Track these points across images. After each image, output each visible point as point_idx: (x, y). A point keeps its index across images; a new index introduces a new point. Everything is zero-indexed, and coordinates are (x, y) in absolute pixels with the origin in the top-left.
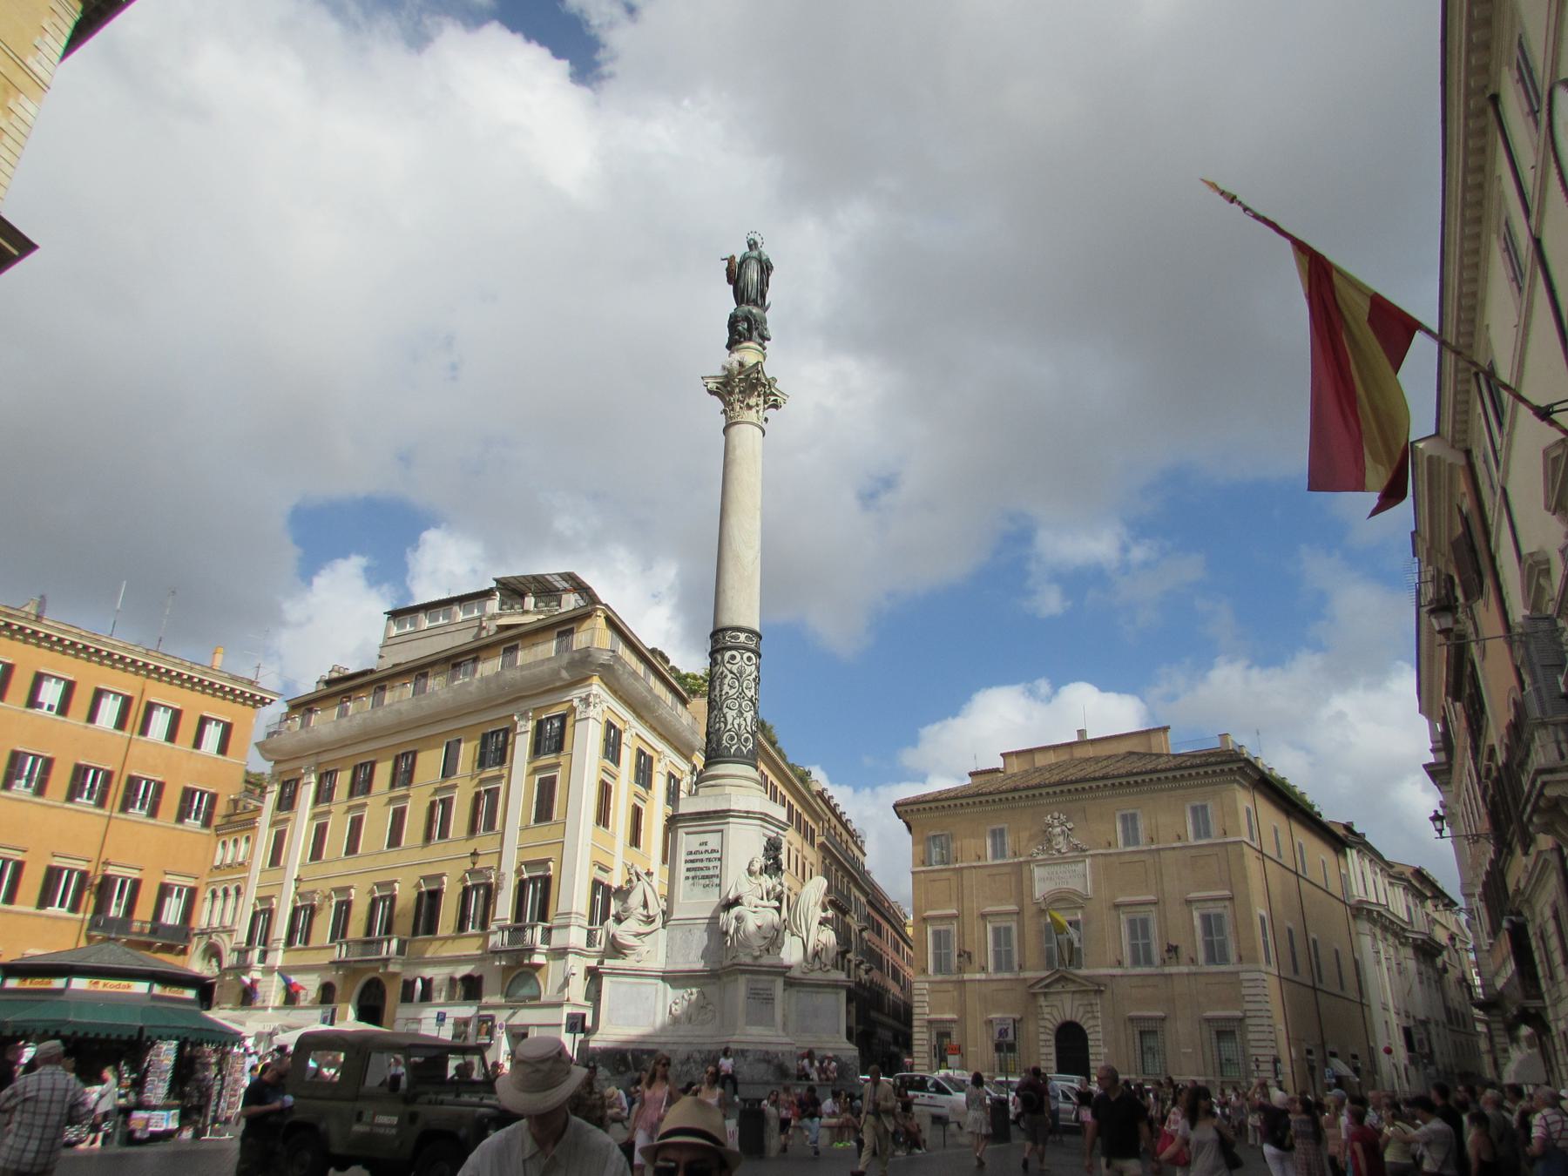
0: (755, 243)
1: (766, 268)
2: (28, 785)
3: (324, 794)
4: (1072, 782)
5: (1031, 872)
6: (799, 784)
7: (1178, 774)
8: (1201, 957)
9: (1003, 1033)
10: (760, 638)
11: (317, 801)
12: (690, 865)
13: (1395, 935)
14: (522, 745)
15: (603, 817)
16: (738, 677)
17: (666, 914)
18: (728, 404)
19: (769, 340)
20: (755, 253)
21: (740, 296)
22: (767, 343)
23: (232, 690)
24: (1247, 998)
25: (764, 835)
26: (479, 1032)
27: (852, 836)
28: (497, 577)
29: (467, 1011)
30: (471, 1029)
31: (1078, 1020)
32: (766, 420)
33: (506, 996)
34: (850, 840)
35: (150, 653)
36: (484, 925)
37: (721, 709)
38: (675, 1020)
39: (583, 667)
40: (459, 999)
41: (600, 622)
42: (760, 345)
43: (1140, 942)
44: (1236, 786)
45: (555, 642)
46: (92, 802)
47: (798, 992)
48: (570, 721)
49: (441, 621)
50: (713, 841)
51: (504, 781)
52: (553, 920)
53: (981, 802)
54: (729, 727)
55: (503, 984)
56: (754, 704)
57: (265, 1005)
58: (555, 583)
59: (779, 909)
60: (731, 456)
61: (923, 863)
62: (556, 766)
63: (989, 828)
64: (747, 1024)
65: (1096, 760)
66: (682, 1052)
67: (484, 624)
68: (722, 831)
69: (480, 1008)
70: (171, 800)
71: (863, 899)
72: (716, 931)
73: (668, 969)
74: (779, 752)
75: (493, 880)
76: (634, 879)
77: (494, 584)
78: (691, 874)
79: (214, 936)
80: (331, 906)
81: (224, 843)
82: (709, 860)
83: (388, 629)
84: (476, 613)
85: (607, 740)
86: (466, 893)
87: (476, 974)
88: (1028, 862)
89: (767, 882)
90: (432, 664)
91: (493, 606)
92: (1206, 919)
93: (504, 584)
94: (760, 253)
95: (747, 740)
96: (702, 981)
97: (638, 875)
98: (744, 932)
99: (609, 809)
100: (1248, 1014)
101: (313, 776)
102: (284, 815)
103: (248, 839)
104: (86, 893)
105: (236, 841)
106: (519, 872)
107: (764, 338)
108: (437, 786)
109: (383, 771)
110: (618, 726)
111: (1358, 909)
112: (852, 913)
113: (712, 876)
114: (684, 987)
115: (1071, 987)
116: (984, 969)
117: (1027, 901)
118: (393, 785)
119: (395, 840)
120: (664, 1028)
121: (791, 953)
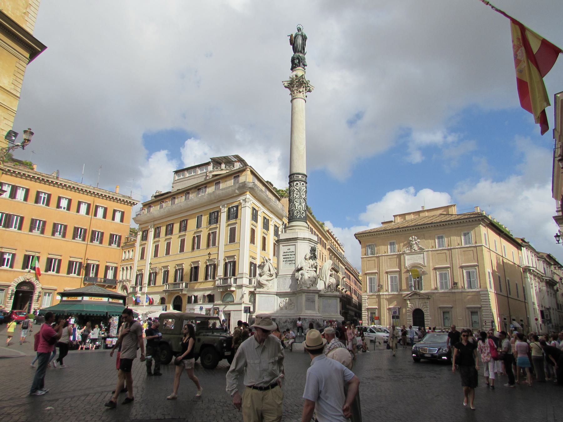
0: (300, 29)
1: (304, 38)
2: (60, 234)
3: (157, 235)
4: (419, 225)
5: (404, 257)
6: (320, 228)
7: (459, 221)
8: (466, 286)
9: (395, 312)
10: (307, 177)
11: (155, 237)
12: (285, 257)
13: (539, 278)
14: (223, 216)
15: (253, 241)
16: (299, 191)
17: (277, 274)
18: (292, 91)
19: (306, 66)
20: (300, 33)
21: (295, 50)
22: (306, 67)
23: (123, 200)
24: (483, 301)
25: (310, 246)
26: (214, 313)
27: (339, 245)
28: (211, 157)
29: (210, 306)
30: (211, 312)
31: (421, 308)
32: (306, 96)
33: (222, 301)
34: (339, 247)
35: (95, 188)
36: (214, 278)
37: (293, 202)
38: (281, 309)
39: (243, 189)
40: (207, 302)
41: (249, 172)
42: (303, 68)
43: (444, 281)
44: (481, 225)
45: (233, 180)
46: (81, 239)
47: (323, 299)
48: (239, 208)
49: (193, 174)
50: (292, 248)
51: (218, 229)
52: (237, 276)
53: (386, 233)
54: (296, 209)
55: (221, 297)
56: (305, 200)
57: (143, 305)
58: (232, 159)
59: (316, 271)
60: (294, 111)
61: (365, 255)
62: (236, 223)
63: (389, 242)
64: (306, 310)
65: (429, 217)
66: (284, 319)
67: (208, 175)
68: (295, 245)
69: (214, 305)
70: (106, 238)
71: (344, 267)
72: (294, 279)
73: (278, 291)
74: (313, 216)
75: (216, 263)
76: (265, 262)
77: (210, 160)
78: (285, 260)
79: (124, 283)
80: (162, 272)
81: (125, 252)
82: (291, 255)
83: (174, 177)
84: (205, 171)
85: (253, 214)
86: (207, 267)
87: (212, 294)
88: (403, 254)
89: (311, 262)
90: (191, 189)
91: (210, 168)
92: (469, 274)
93: (214, 160)
94: (302, 33)
95: (303, 213)
96: (290, 295)
97: (266, 260)
98: (304, 279)
99: (255, 238)
100: (483, 306)
101: (153, 228)
102: (144, 242)
103: (133, 250)
104: (82, 269)
105: (129, 251)
106: (225, 260)
107: (305, 65)
108: (195, 231)
109: (176, 227)
110: (256, 209)
111: (525, 269)
112: (340, 272)
113: (292, 260)
114: (284, 297)
115: (418, 297)
116: (387, 291)
117: (403, 267)
118: (180, 231)
119: (182, 250)
120: (277, 311)
121: (320, 286)
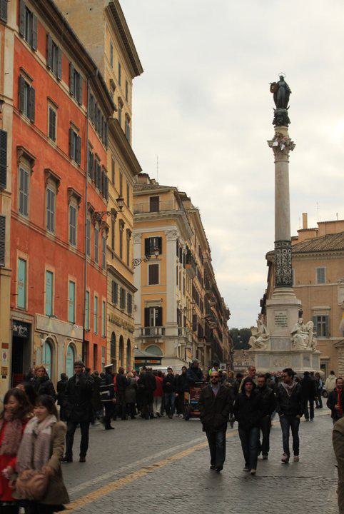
1: (288, 92)
20: (283, 83)
37: (282, 269)
50: (284, 313)
52: (165, 325)
63: (316, 268)
